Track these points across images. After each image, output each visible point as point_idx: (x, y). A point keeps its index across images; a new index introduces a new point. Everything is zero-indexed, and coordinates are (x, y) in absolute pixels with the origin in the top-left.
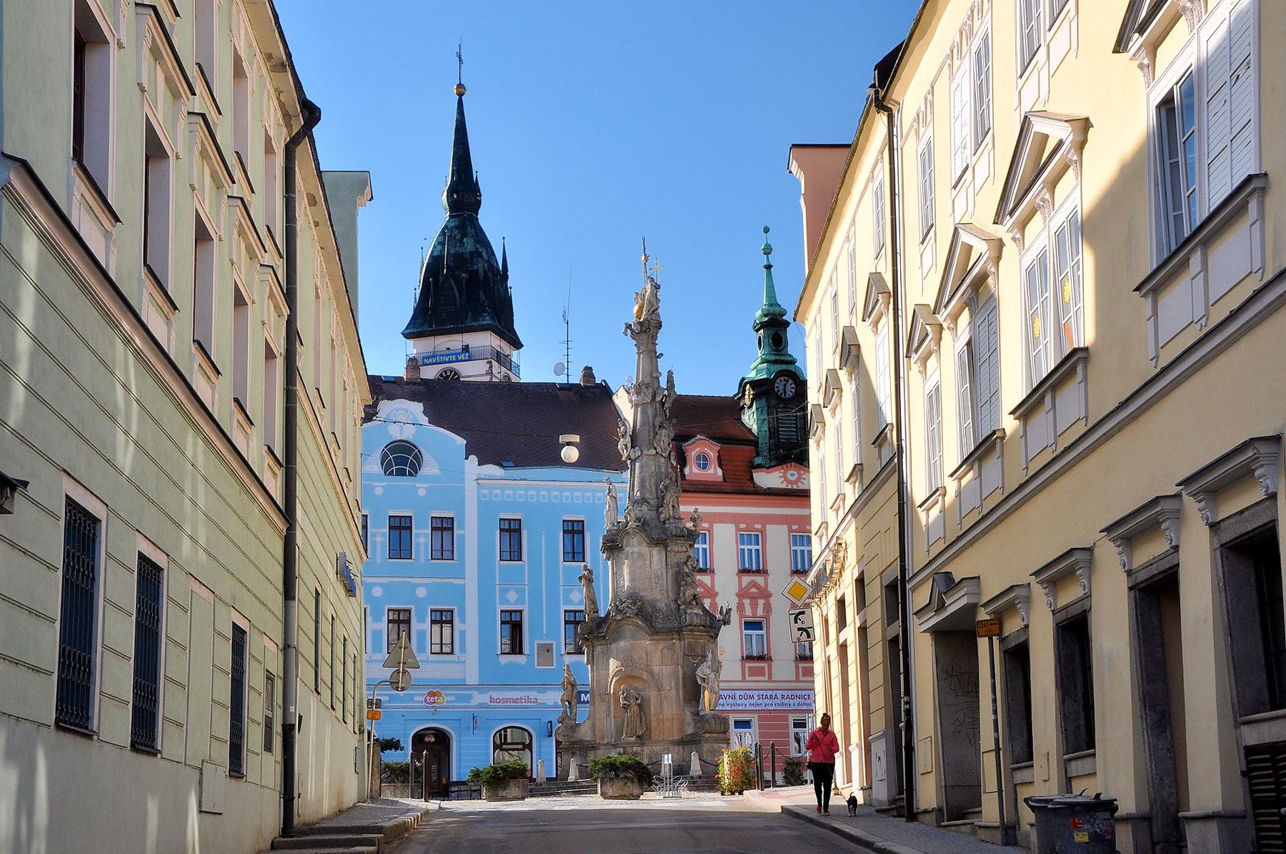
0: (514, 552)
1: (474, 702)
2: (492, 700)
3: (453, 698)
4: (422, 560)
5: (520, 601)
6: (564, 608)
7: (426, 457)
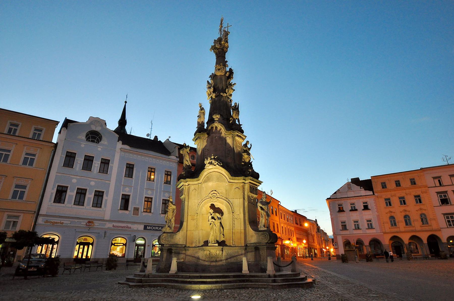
2: (113, 226)
3: (98, 224)
4: (95, 172)
5: (130, 191)
6: (145, 196)
7: (104, 138)
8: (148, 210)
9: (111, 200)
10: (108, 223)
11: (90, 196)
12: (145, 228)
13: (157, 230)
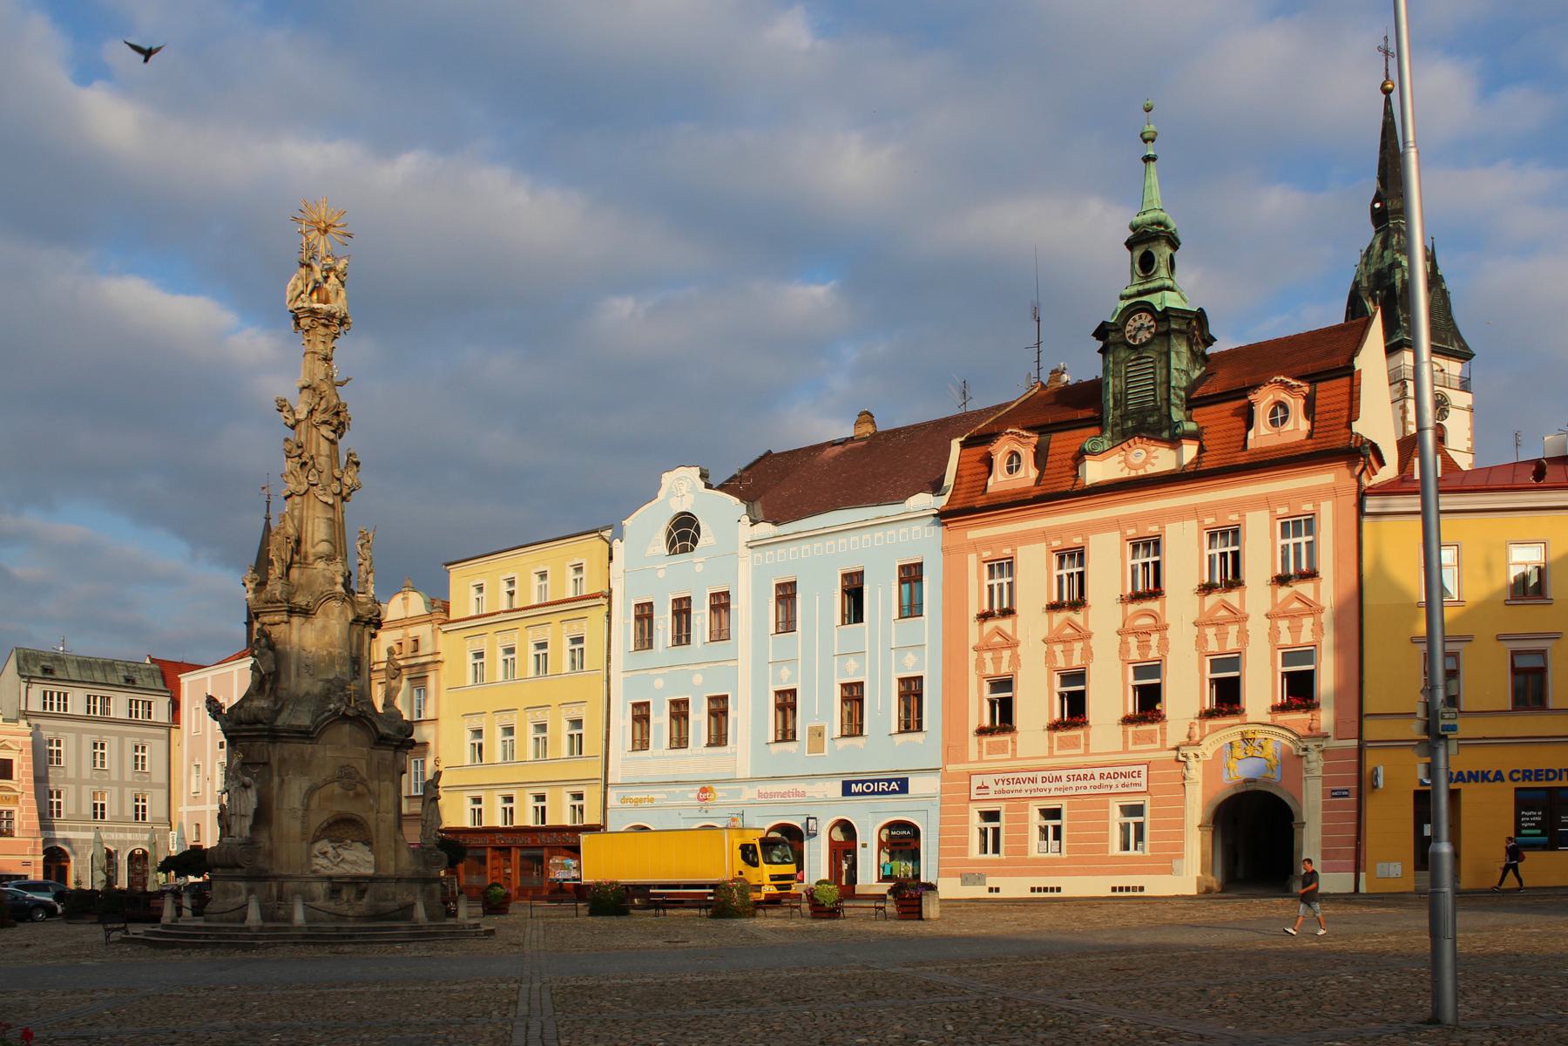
0: (787, 624)
1: (743, 799)
2: (760, 795)
4: (699, 644)
8: (854, 725)
9: (751, 717)
10: (745, 787)
11: (699, 717)
12: (847, 789)
13: (884, 792)
